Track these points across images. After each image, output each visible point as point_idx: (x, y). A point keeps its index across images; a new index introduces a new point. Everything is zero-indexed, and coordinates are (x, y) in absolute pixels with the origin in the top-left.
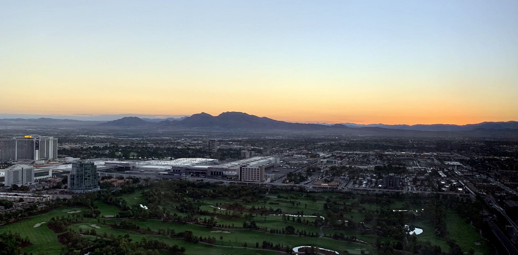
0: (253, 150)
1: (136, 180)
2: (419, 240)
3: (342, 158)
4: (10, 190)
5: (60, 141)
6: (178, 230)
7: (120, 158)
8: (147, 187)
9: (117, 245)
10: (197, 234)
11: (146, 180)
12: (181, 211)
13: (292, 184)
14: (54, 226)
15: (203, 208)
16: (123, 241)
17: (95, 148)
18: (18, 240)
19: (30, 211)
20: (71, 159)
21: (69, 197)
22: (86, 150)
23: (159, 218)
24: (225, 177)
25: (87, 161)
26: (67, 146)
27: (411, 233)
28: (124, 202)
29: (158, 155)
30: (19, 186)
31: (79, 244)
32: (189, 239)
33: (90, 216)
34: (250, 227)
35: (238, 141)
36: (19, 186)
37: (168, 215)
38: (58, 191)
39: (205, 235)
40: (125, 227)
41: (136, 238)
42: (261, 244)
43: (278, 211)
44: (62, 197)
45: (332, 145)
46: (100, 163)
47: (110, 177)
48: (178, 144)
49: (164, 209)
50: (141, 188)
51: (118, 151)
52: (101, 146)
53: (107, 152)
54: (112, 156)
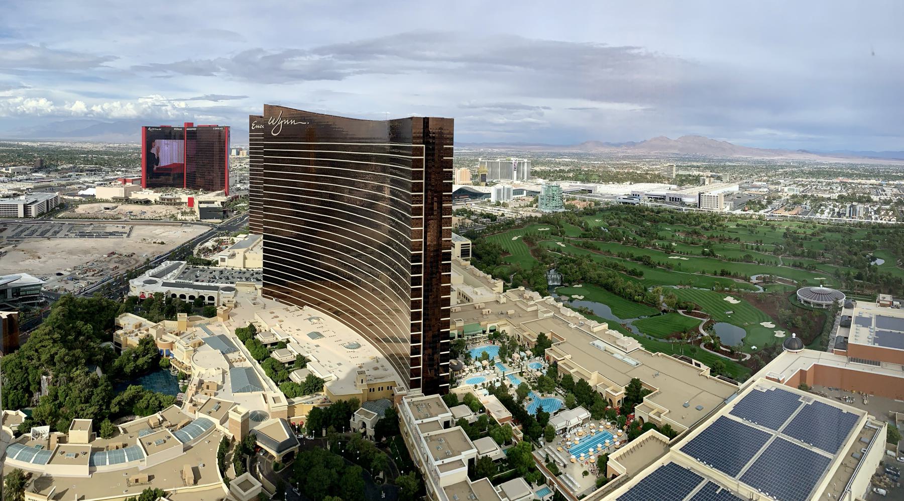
0: (712, 176)
1: (597, 204)
2: (879, 270)
3: (803, 185)
4: (495, 206)
5: (533, 164)
6: (638, 253)
7: (583, 181)
8: (607, 209)
9: (580, 264)
10: (655, 259)
11: (607, 204)
12: (641, 235)
13: (751, 212)
14: (528, 240)
15: (661, 234)
16: (586, 262)
17: (561, 171)
18: (500, 249)
19: (510, 225)
20: (540, 181)
21: (539, 215)
22: (553, 172)
23: (619, 241)
24: (683, 204)
25: (554, 183)
26: (537, 169)
27: (872, 263)
28: (586, 224)
29: (617, 179)
30: (502, 202)
31: (547, 260)
32: (648, 263)
33: (557, 234)
34: (708, 255)
35: (698, 167)
36: (502, 202)
37: (627, 239)
38: (530, 209)
39: (663, 259)
40: (587, 246)
41: (597, 257)
42: (719, 272)
43: (737, 239)
44: (534, 215)
45: (793, 172)
46: (565, 185)
47: (574, 199)
48: (637, 168)
49: (624, 232)
50: (601, 210)
51: (580, 174)
52: (567, 169)
53: (571, 175)
54: (576, 179)
